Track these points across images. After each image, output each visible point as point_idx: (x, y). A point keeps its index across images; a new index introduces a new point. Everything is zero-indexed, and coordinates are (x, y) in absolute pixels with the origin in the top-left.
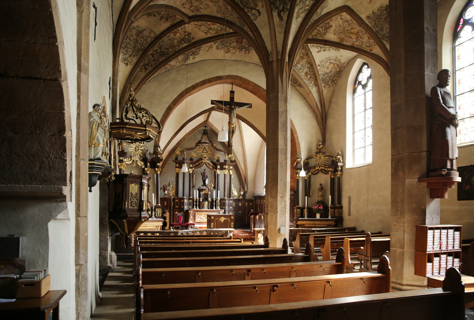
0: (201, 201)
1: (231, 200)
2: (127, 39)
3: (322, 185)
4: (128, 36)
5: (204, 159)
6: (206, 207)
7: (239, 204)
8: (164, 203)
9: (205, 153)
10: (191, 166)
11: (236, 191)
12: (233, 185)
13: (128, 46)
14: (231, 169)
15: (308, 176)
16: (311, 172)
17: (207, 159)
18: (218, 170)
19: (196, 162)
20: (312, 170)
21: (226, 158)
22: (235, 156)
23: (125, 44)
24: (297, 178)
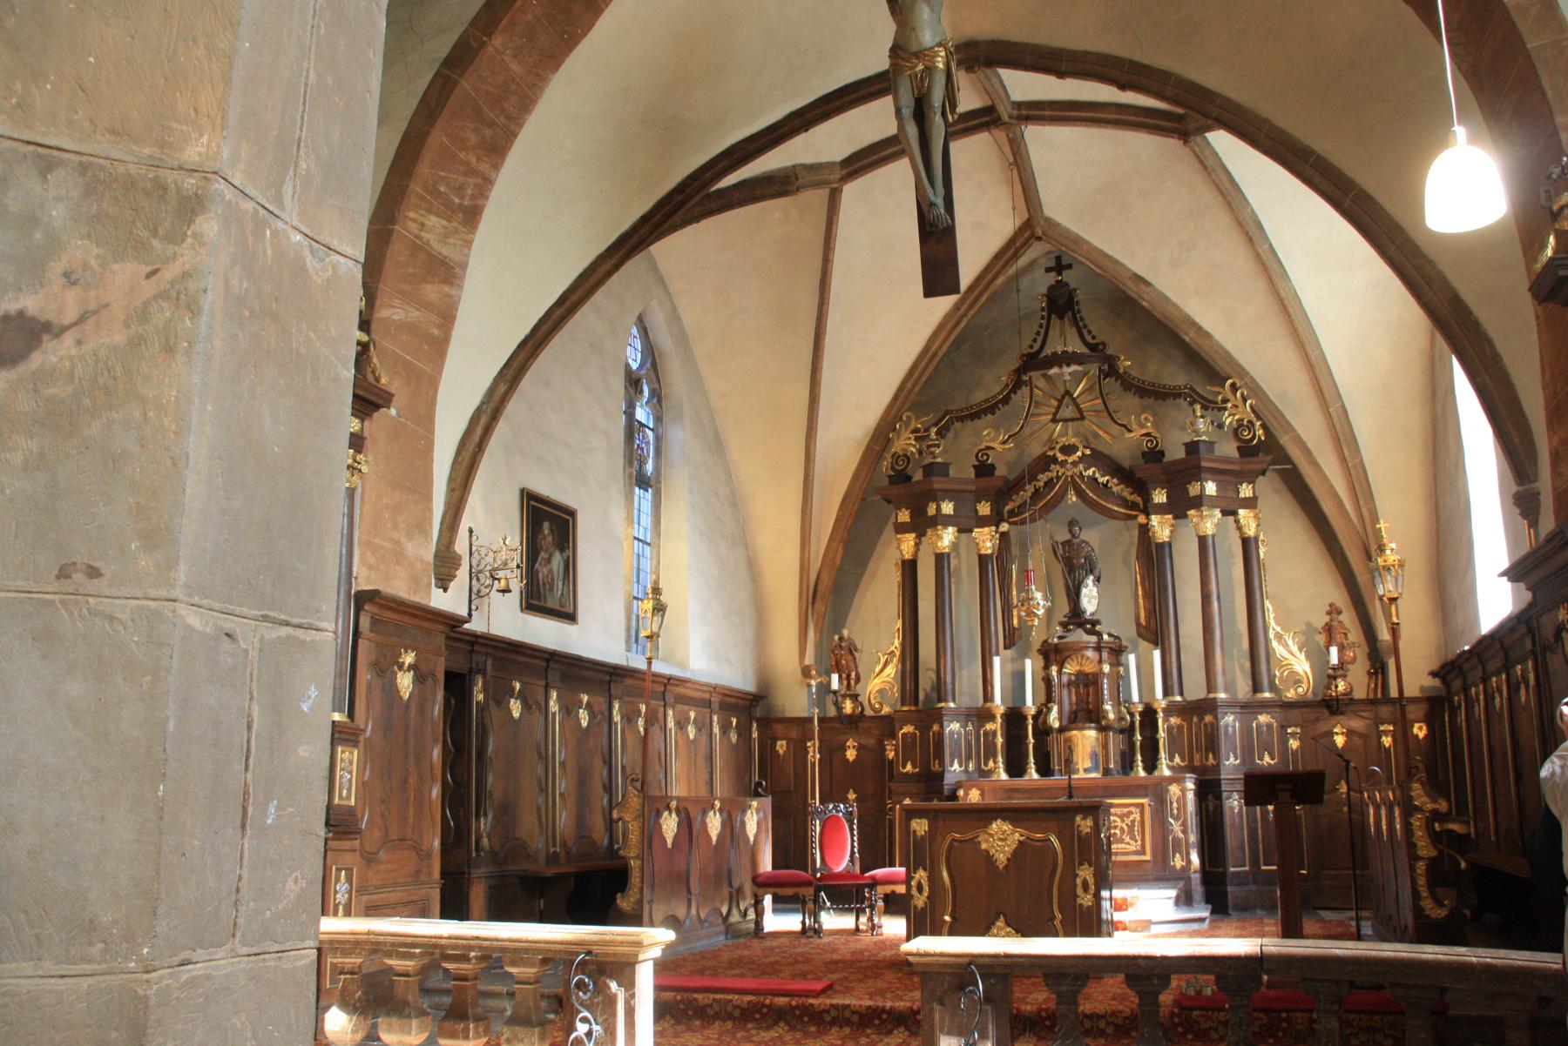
0: (1056, 725)
1: (1265, 706)
5: (1060, 457)
6: (1088, 764)
7: (1331, 734)
8: (844, 749)
9: (1065, 420)
10: (984, 509)
11: (1295, 649)
12: (1267, 604)
14: (1250, 503)
17: (1081, 459)
18: (1153, 517)
19: (1014, 486)
21: (1196, 432)
22: (1265, 411)
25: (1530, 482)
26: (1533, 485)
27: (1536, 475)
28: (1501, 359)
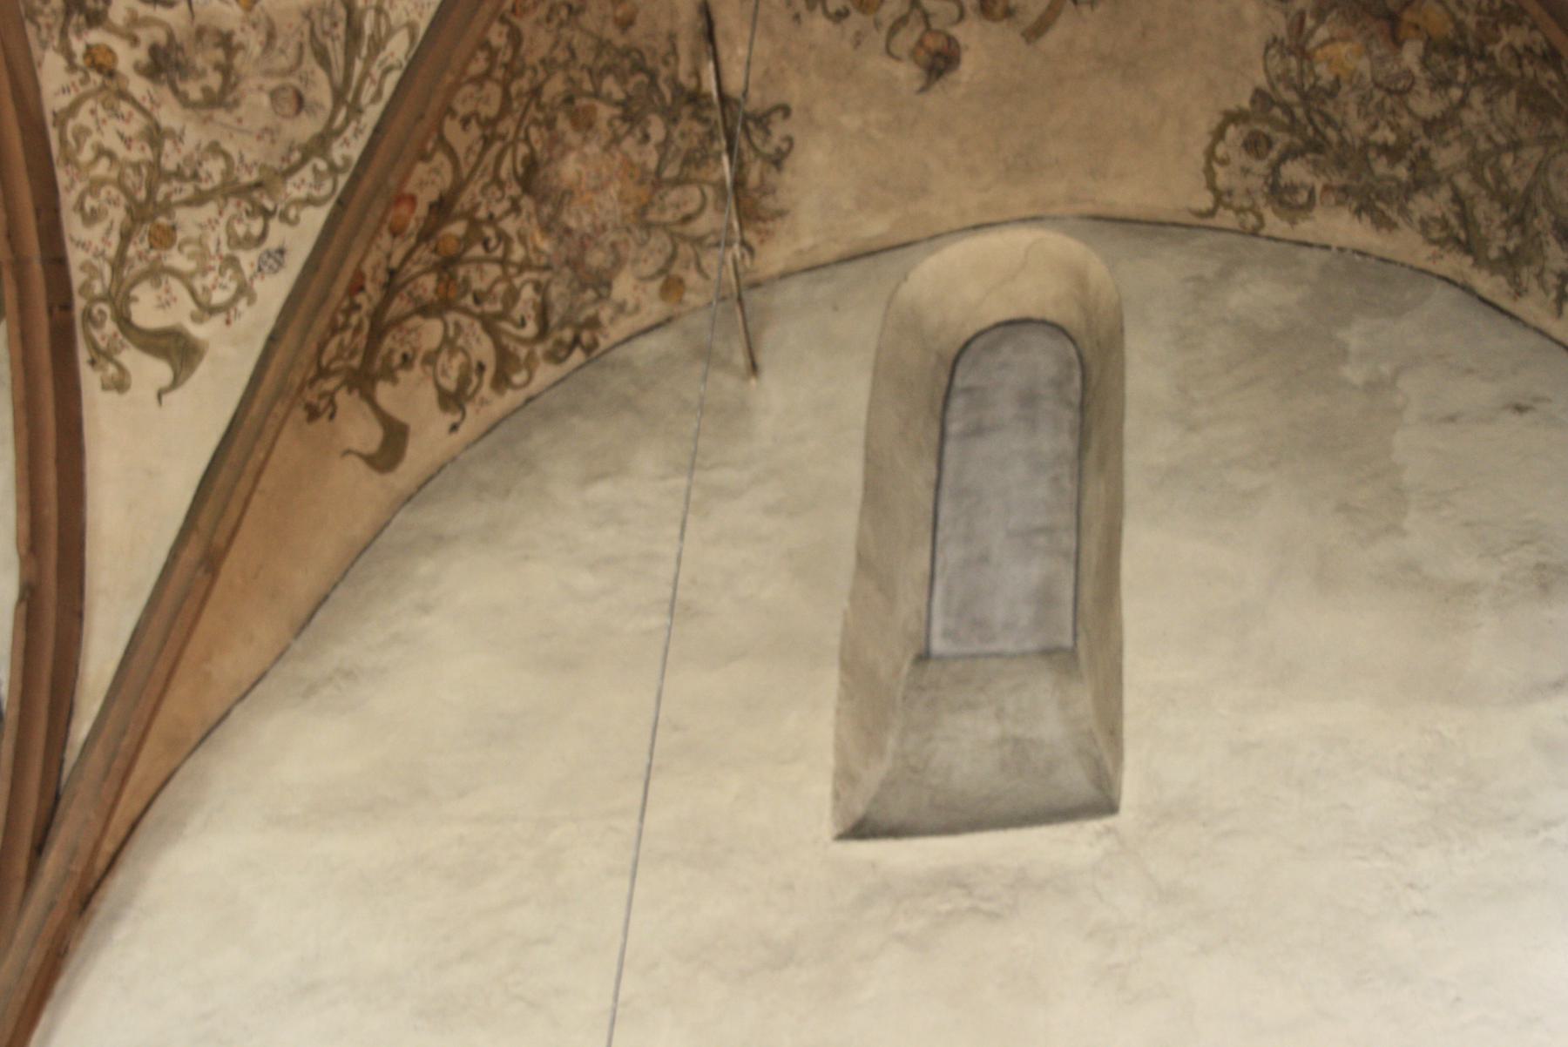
2: (1424, 154)
4: (1386, 135)
13: (1517, 183)
23: (1485, 210)
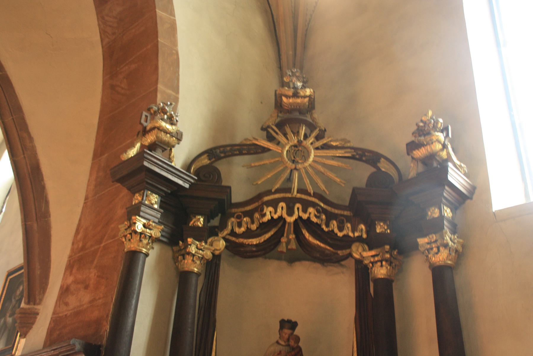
3: (297, 332)
15: (208, 254)
16: (226, 232)
20: (233, 220)
24: (132, 245)
25: (34, 304)
26: (36, 307)
27: (41, 300)
28: (50, 217)
